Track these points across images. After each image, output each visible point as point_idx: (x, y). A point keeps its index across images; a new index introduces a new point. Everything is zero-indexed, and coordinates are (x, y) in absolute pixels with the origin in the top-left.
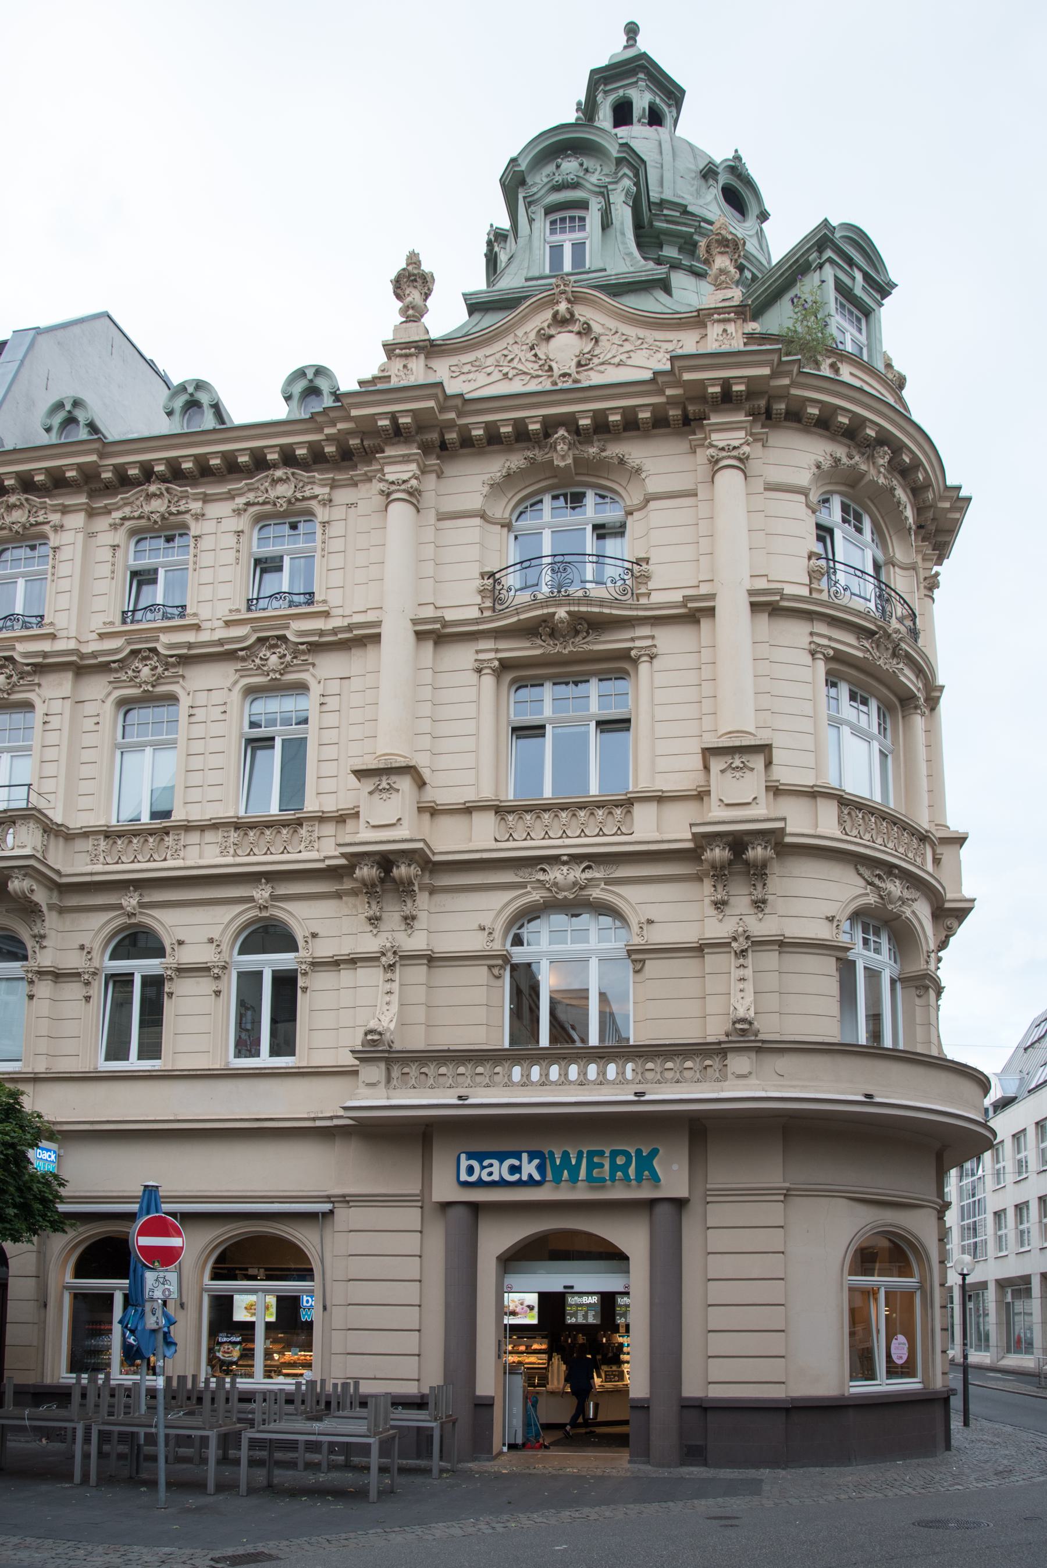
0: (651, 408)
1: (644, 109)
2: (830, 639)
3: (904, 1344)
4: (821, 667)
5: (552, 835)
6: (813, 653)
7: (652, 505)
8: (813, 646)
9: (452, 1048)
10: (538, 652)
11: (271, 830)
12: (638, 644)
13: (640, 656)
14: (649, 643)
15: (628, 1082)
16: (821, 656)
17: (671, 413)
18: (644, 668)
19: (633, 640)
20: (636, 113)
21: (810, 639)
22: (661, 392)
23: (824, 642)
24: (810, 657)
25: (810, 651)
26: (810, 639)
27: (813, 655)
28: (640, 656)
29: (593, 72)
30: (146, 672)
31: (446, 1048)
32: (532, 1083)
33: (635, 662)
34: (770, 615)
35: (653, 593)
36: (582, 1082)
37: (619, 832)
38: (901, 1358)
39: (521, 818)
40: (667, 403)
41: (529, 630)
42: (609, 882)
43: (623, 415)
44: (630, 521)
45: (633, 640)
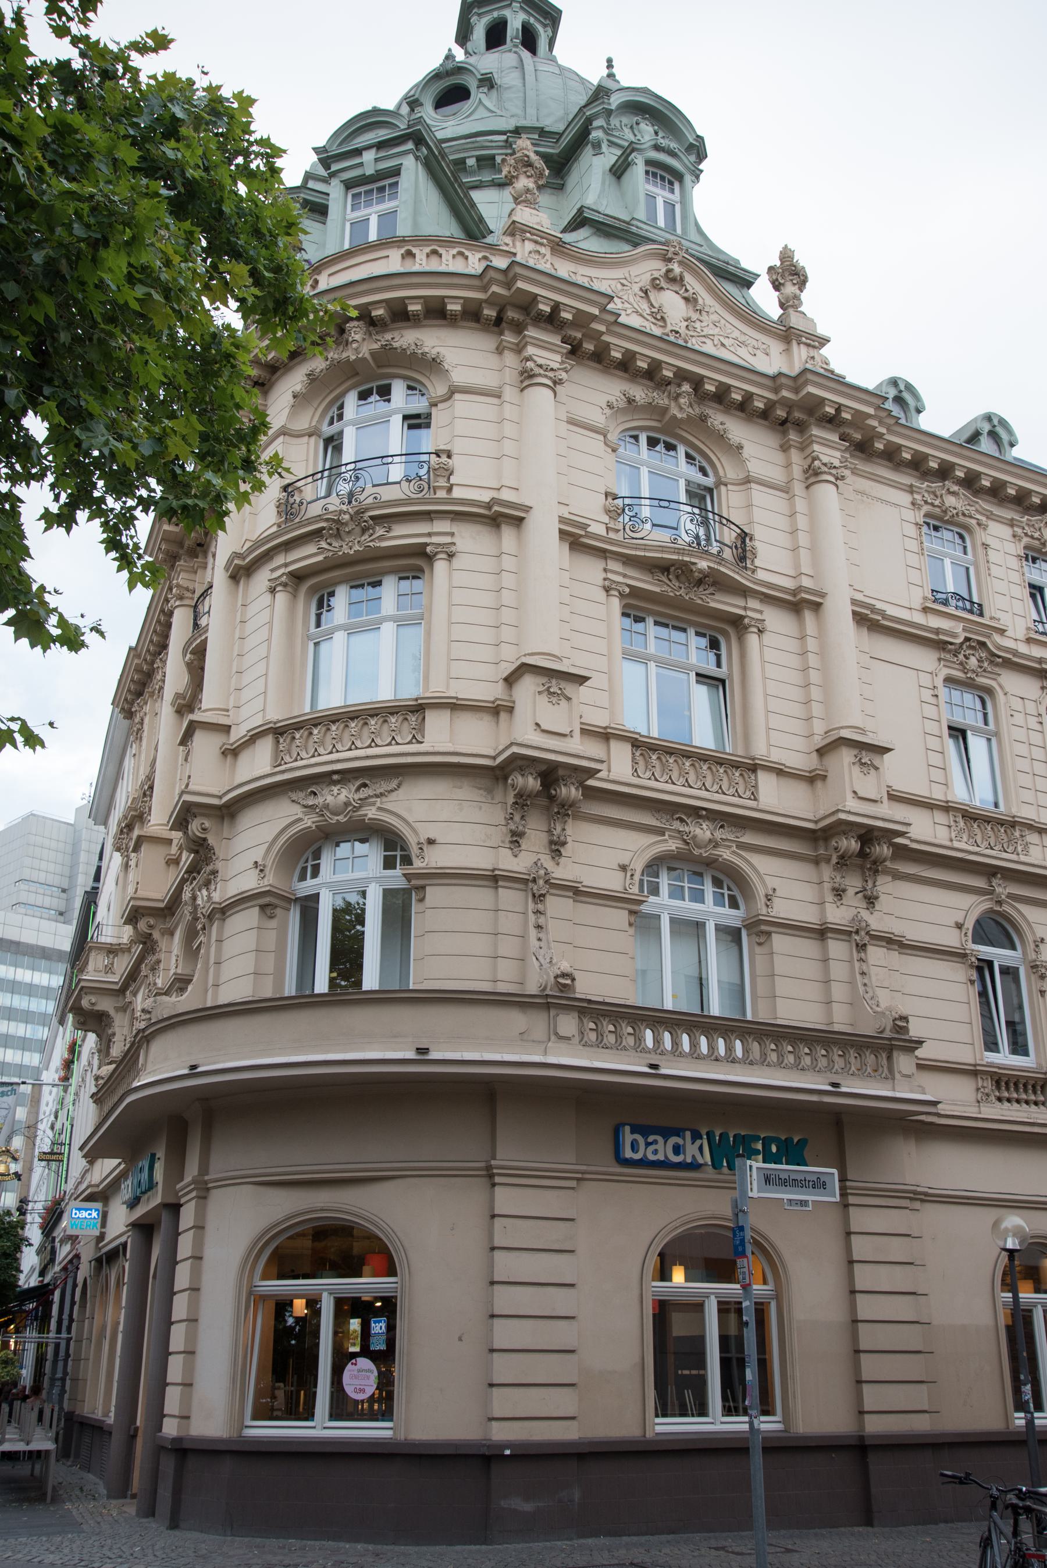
0: (462, 301)
1: (517, 29)
2: (625, 576)
3: (371, 1371)
4: (616, 604)
5: (399, 740)
6: (607, 590)
7: (457, 396)
8: (607, 583)
9: (607, 1000)
10: (657, 589)
11: (376, 719)
12: (435, 540)
13: (437, 553)
14: (447, 539)
15: (645, 1050)
16: (617, 593)
17: (486, 312)
18: (440, 566)
19: (429, 535)
20: (510, 32)
21: (604, 575)
22: (485, 289)
23: (619, 579)
24: (604, 593)
25: (604, 587)
26: (604, 575)
27: (607, 591)
28: (437, 553)
29: (561, 12)
30: (973, 661)
31: (600, 999)
32: (682, 1055)
33: (430, 558)
34: (571, 544)
35: (455, 488)
36: (713, 1057)
37: (415, 740)
38: (363, 1391)
39: (406, 719)
40: (486, 301)
41: (662, 568)
42: (742, 846)
43: (463, 306)
44: (434, 411)
45: (429, 535)
